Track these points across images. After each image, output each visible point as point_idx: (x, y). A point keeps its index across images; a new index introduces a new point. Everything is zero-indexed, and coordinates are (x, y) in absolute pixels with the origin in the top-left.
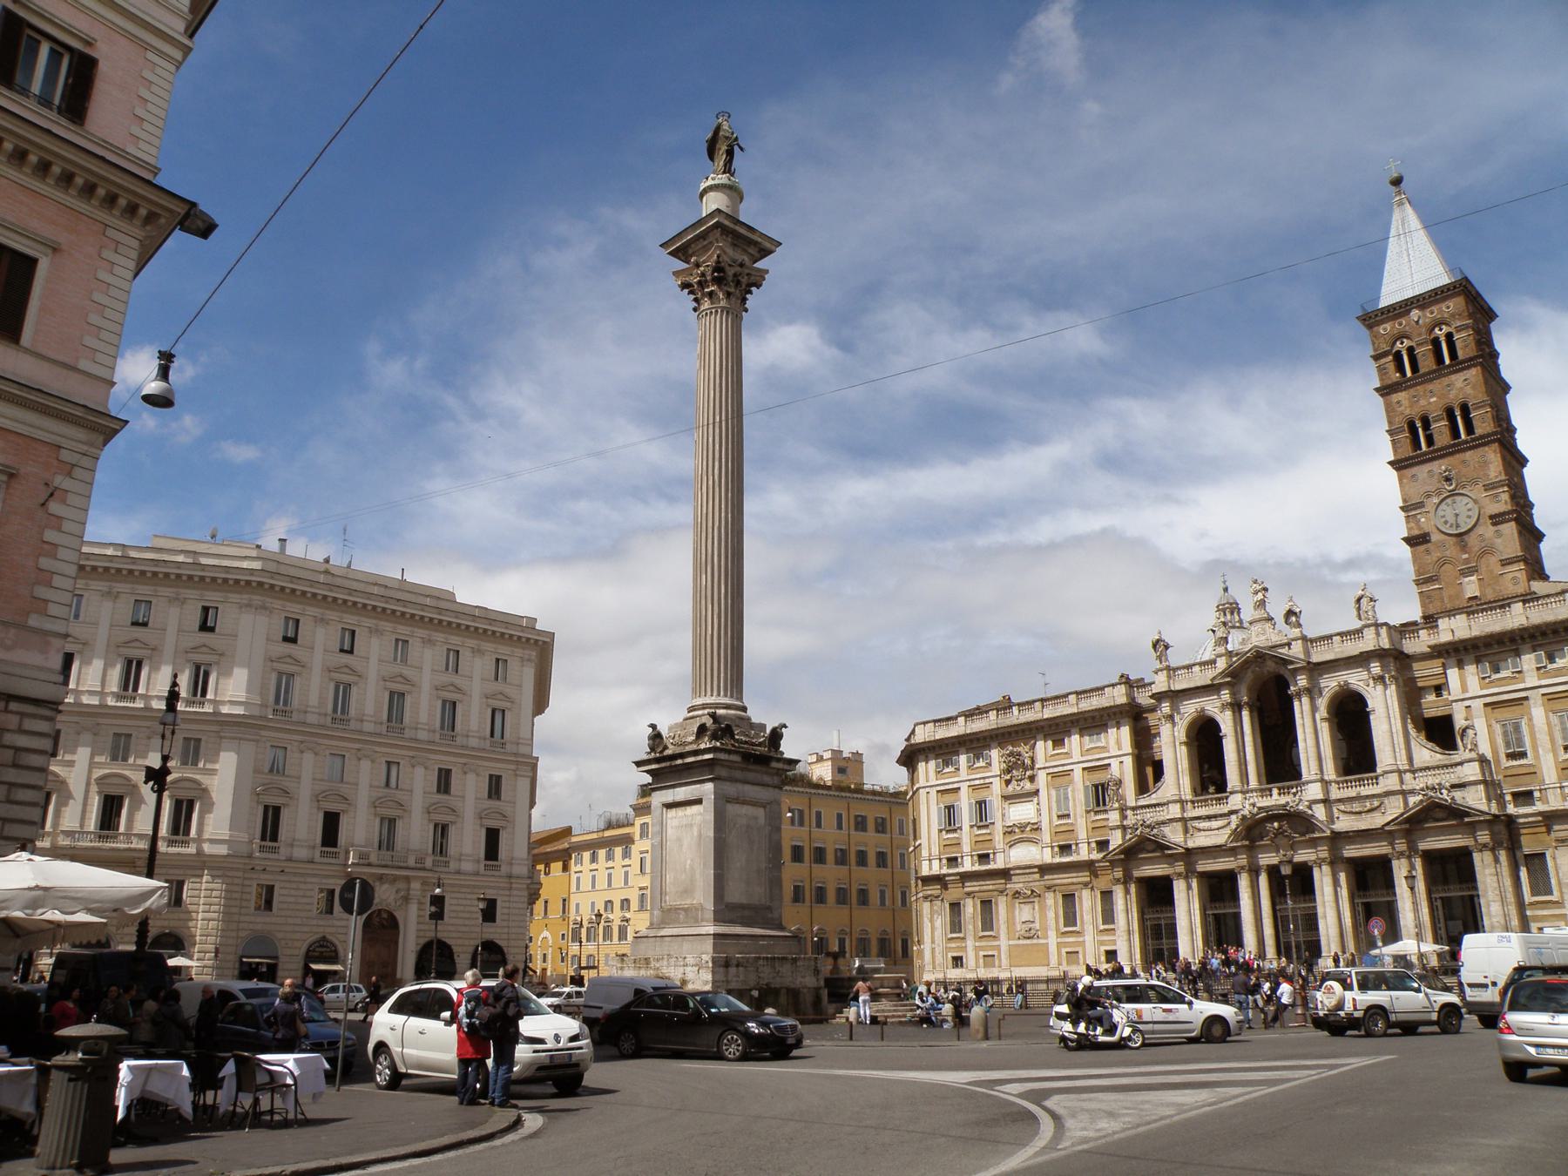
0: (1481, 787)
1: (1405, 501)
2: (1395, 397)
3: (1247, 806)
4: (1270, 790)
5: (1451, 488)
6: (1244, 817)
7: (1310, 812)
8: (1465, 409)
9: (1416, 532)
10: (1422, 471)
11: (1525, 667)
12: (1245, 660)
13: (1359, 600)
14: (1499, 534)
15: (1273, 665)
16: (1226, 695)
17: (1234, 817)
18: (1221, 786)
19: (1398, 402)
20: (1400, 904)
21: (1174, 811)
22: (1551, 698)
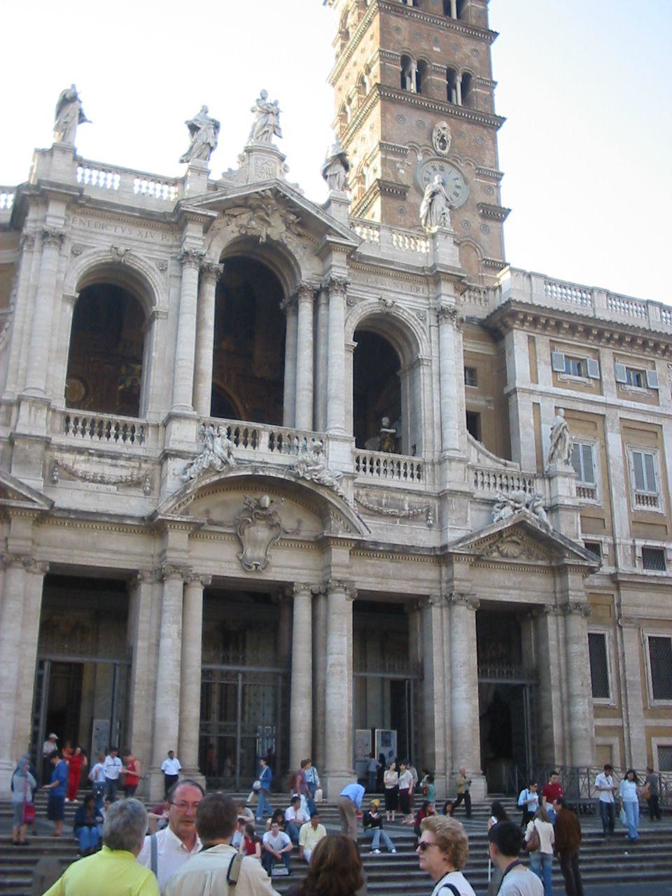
0: (577, 518)
1: (383, 138)
2: (395, 21)
3: (219, 449)
4: (255, 434)
5: (445, 152)
6: (211, 469)
7: (341, 491)
8: (466, 78)
9: (394, 181)
10: (414, 117)
11: (605, 377)
12: (246, 198)
13: (433, 194)
14: (485, 229)
15: (285, 228)
16: (194, 238)
17: (175, 465)
18: (131, 402)
19: (398, 29)
20: (438, 686)
21: (31, 422)
22: (629, 428)
